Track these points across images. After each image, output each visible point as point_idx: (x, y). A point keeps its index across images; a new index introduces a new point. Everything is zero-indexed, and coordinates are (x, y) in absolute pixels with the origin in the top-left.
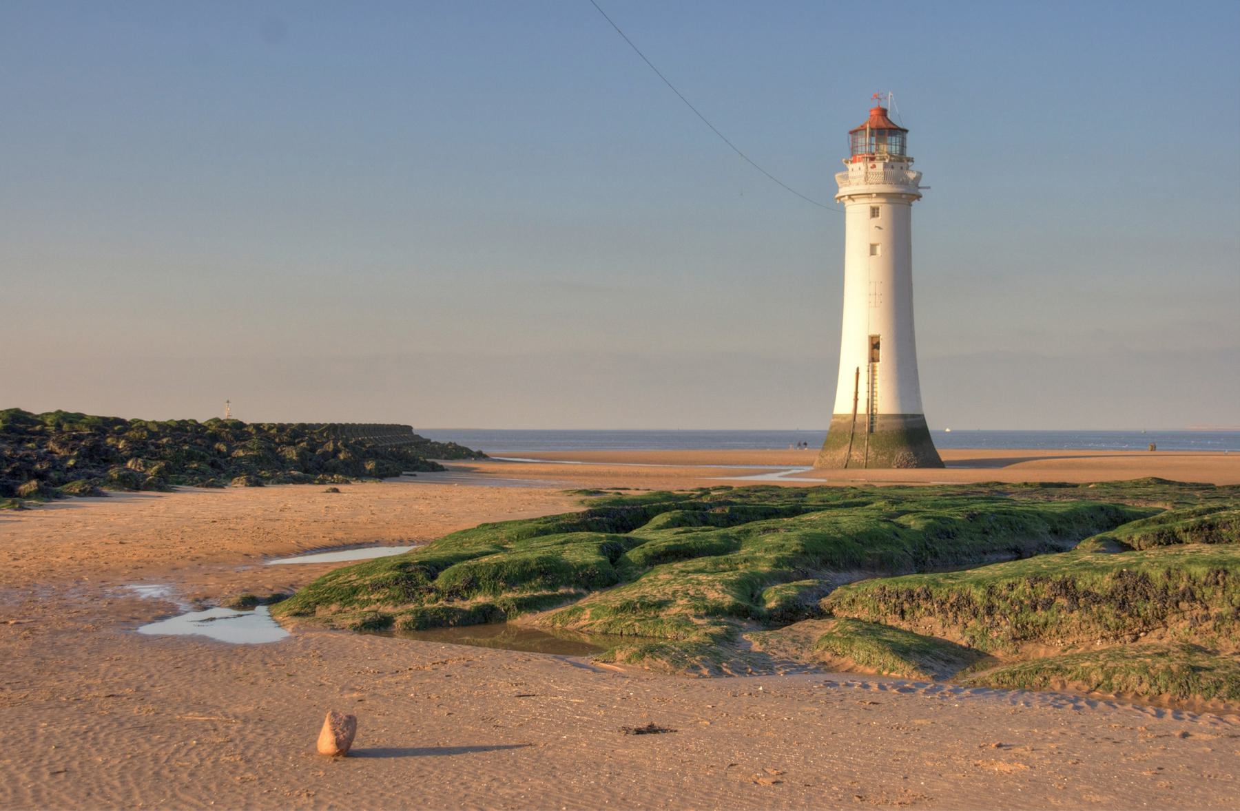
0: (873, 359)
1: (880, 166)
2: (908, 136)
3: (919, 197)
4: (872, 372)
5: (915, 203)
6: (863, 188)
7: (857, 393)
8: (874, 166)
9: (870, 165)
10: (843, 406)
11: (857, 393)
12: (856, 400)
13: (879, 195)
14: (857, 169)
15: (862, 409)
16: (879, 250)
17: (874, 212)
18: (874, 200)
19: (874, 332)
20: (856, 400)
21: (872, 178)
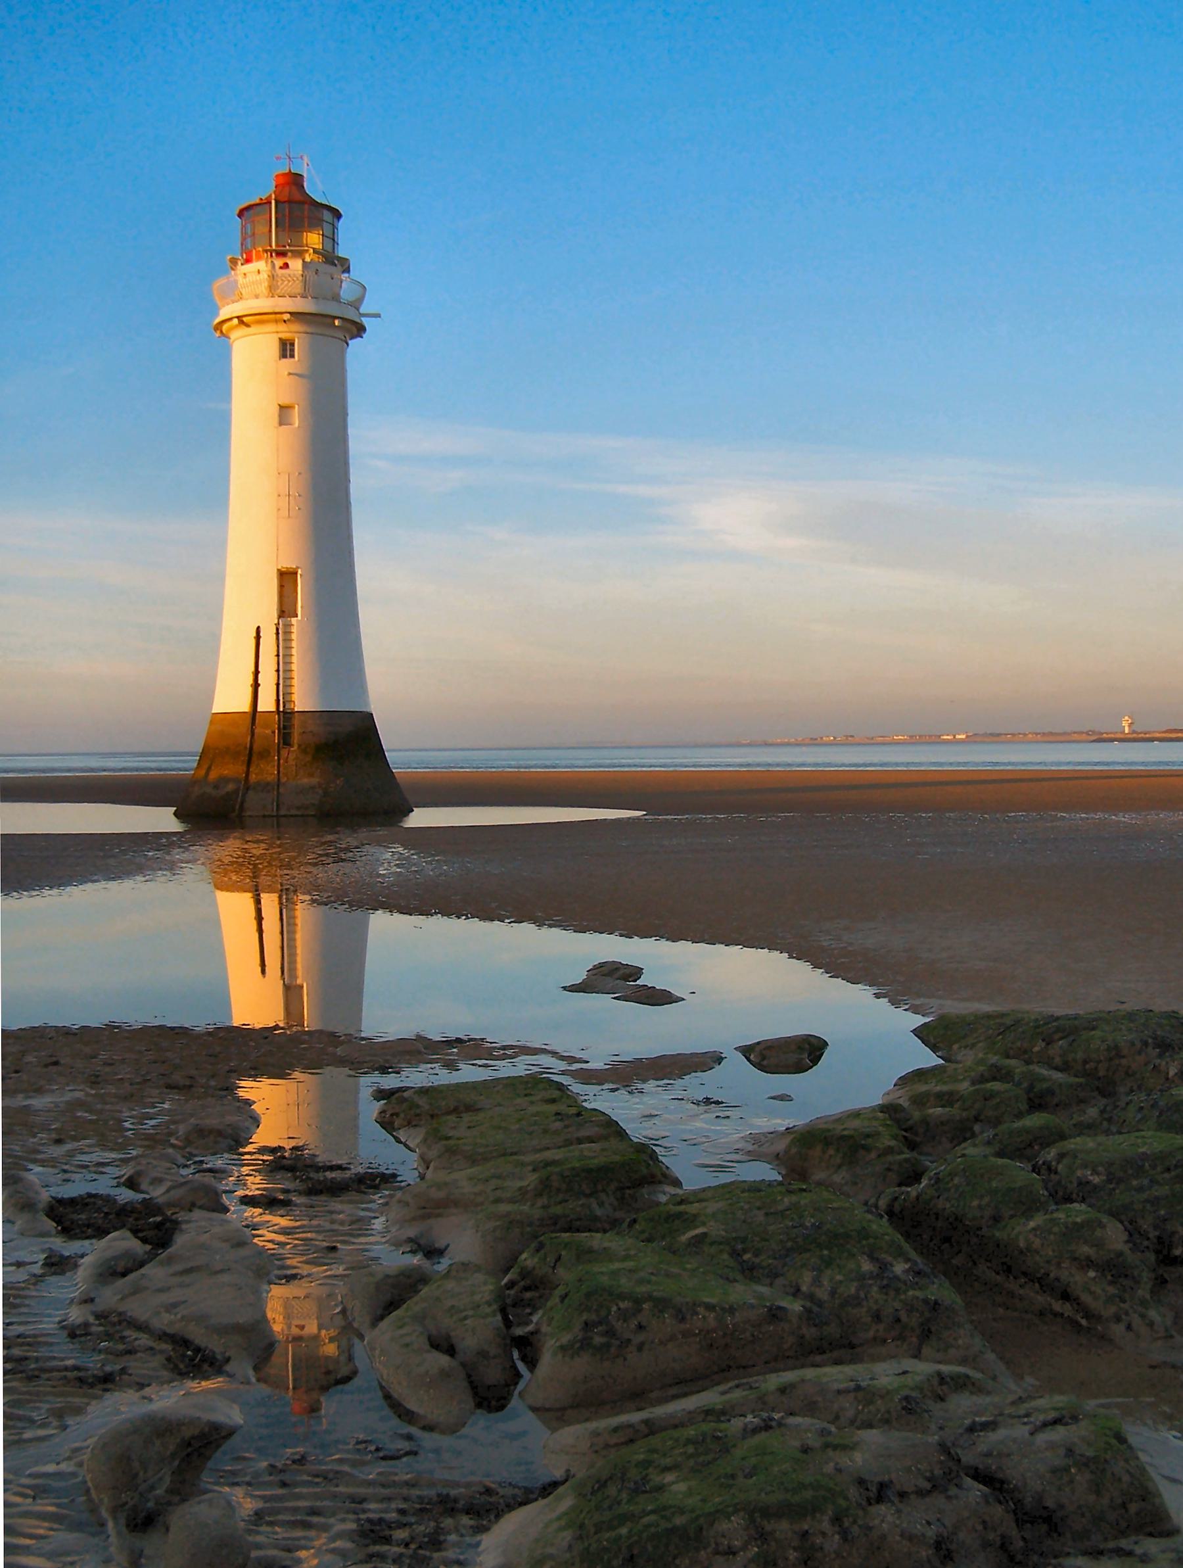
0: (285, 610)
1: (296, 265)
2: (341, 224)
3: (360, 330)
4: (283, 635)
5: (354, 343)
6: (265, 304)
7: (257, 673)
8: (286, 266)
9: (279, 262)
10: (231, 698)
11: (257, 673)
12: (256, 685)
13: (297, 316)
14: (256, 272)
15: (267, 703)
16: (296, 417)
17: (286, 348)
18: (282, 327)
19: (287, 564)
20: (256, 685)
21: (284, 287)
